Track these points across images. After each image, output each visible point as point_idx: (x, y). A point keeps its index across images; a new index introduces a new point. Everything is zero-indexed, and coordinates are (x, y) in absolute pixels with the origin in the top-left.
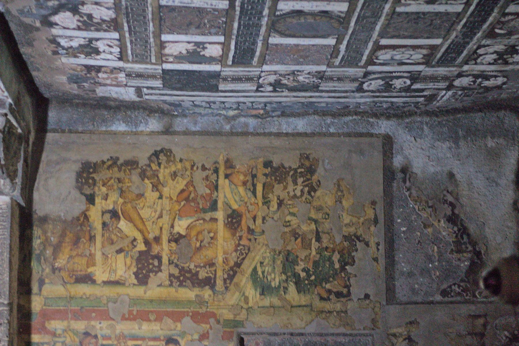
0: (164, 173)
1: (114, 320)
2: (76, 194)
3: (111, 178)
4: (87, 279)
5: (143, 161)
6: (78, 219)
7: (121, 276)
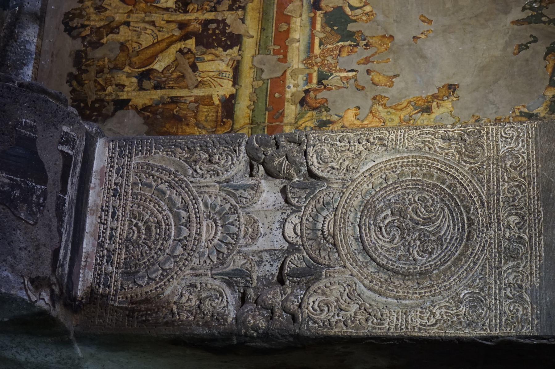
0: (96, 21)
1: (285, 71)
2: (111, 124)
3: (95, 81)
4: (229, 105)
5: (78, 45)
6: (146, 118)
7: (228, 65)
